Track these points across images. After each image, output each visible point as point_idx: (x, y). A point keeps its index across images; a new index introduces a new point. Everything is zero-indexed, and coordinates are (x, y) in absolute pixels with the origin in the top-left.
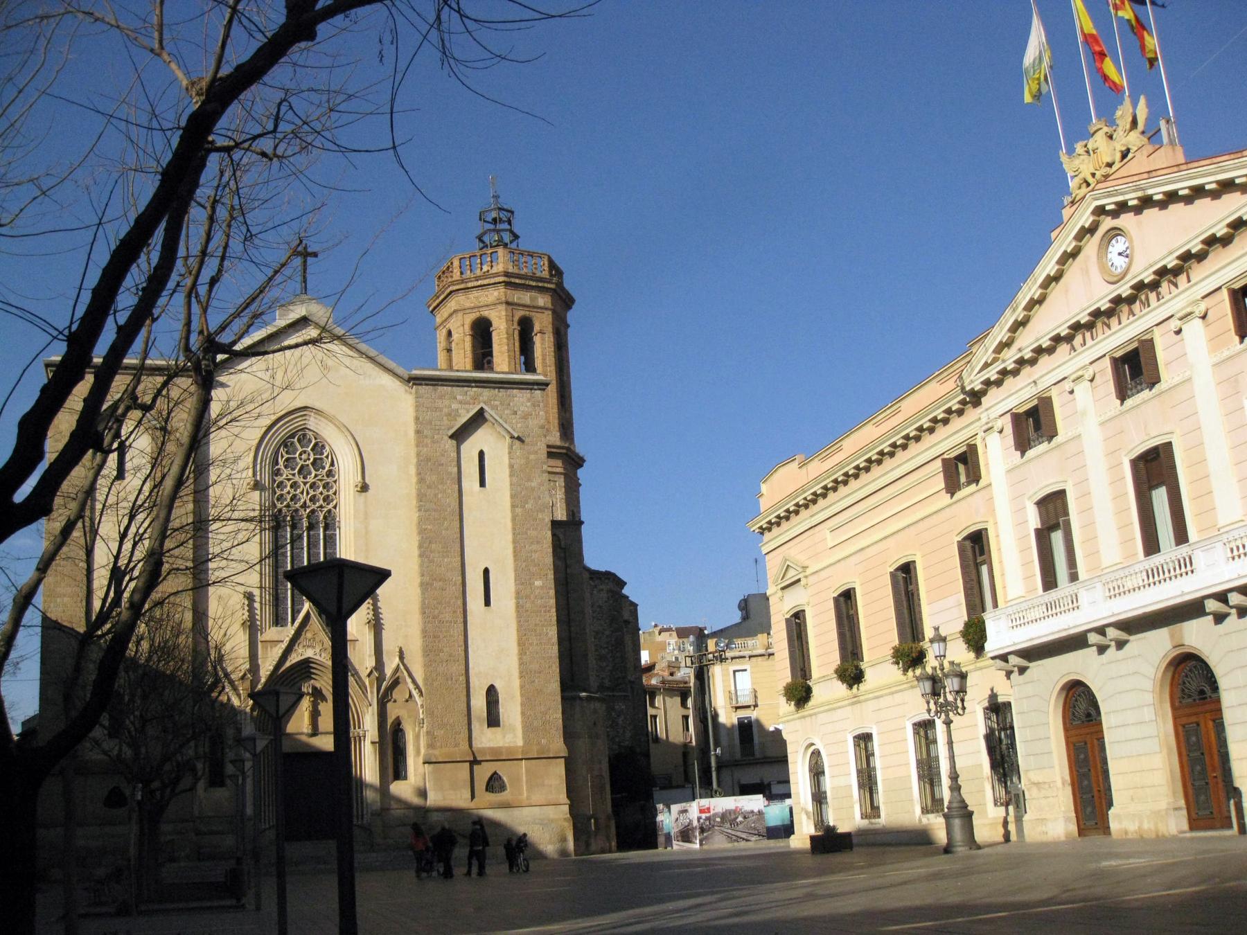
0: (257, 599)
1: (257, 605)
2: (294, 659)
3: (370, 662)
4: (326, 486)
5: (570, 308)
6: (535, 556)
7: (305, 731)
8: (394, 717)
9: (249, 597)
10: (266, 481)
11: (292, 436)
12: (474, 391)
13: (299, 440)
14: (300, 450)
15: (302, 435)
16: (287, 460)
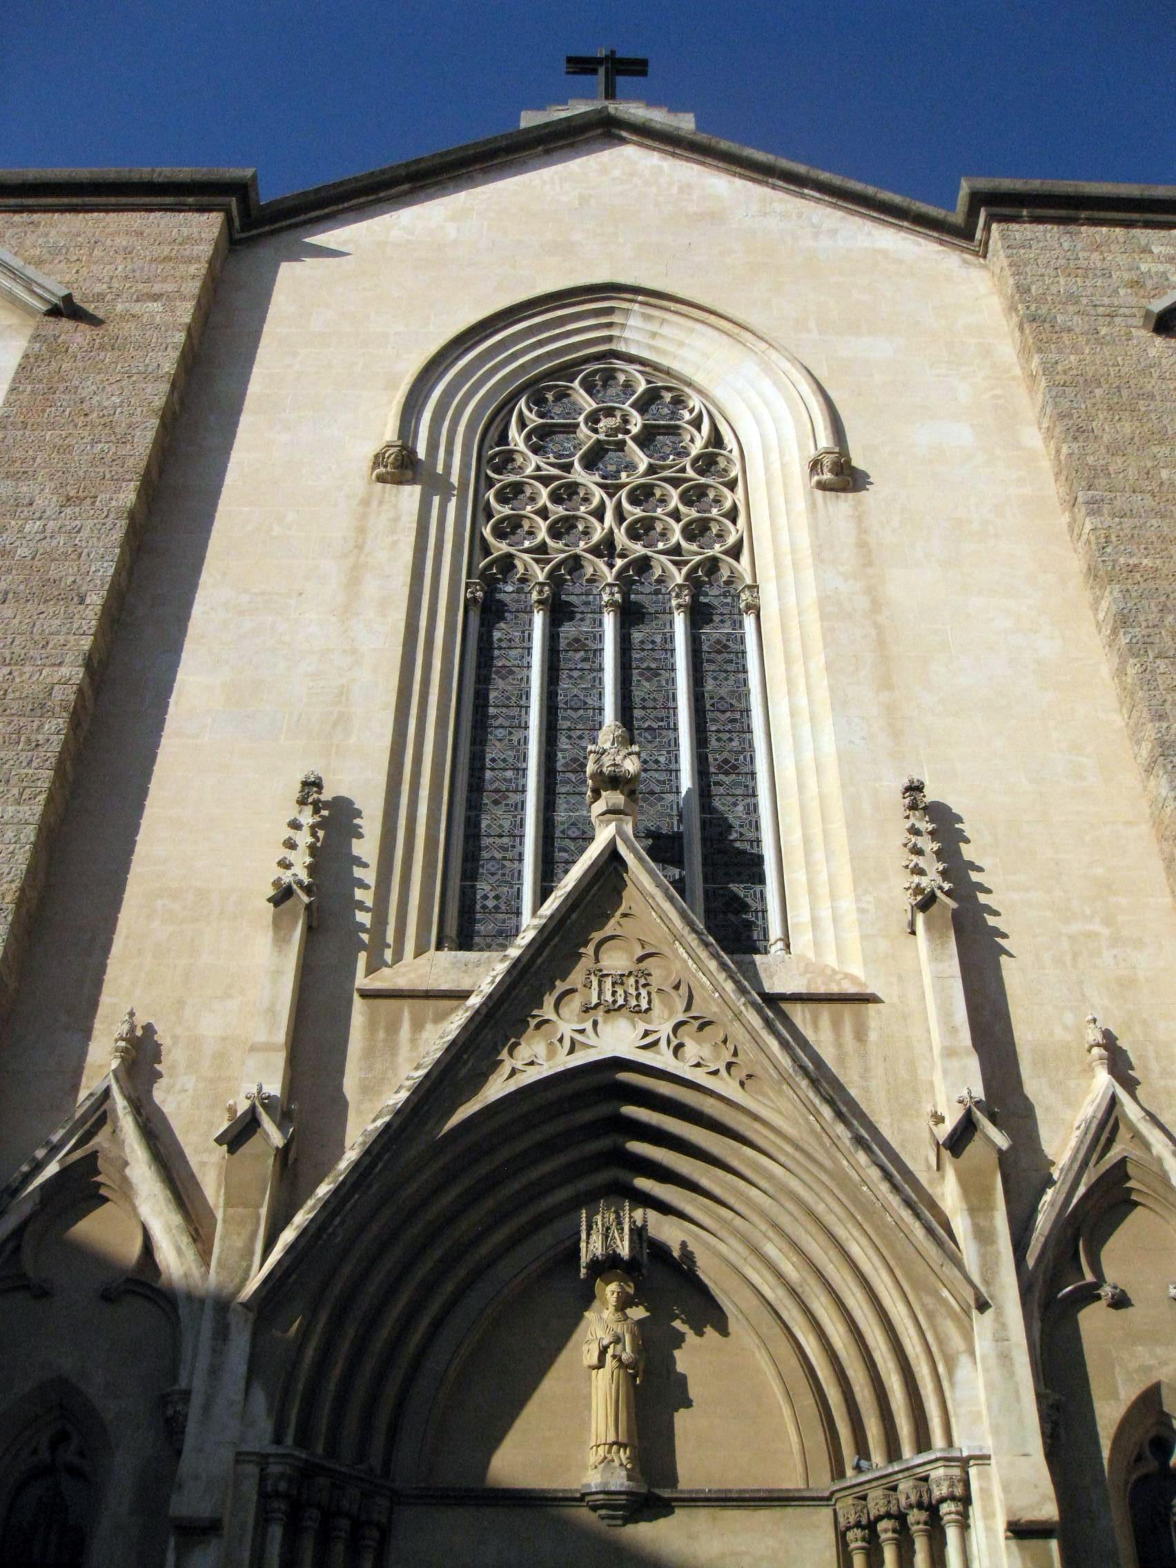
0: (371, 825)
1: (366, 847)
2: (534, 1060)
3: (954, 1083)
7: (593, 1479)
8: (1128, 1394)
9: (336, 820)
10: (455, 464)
11: (567, 371)
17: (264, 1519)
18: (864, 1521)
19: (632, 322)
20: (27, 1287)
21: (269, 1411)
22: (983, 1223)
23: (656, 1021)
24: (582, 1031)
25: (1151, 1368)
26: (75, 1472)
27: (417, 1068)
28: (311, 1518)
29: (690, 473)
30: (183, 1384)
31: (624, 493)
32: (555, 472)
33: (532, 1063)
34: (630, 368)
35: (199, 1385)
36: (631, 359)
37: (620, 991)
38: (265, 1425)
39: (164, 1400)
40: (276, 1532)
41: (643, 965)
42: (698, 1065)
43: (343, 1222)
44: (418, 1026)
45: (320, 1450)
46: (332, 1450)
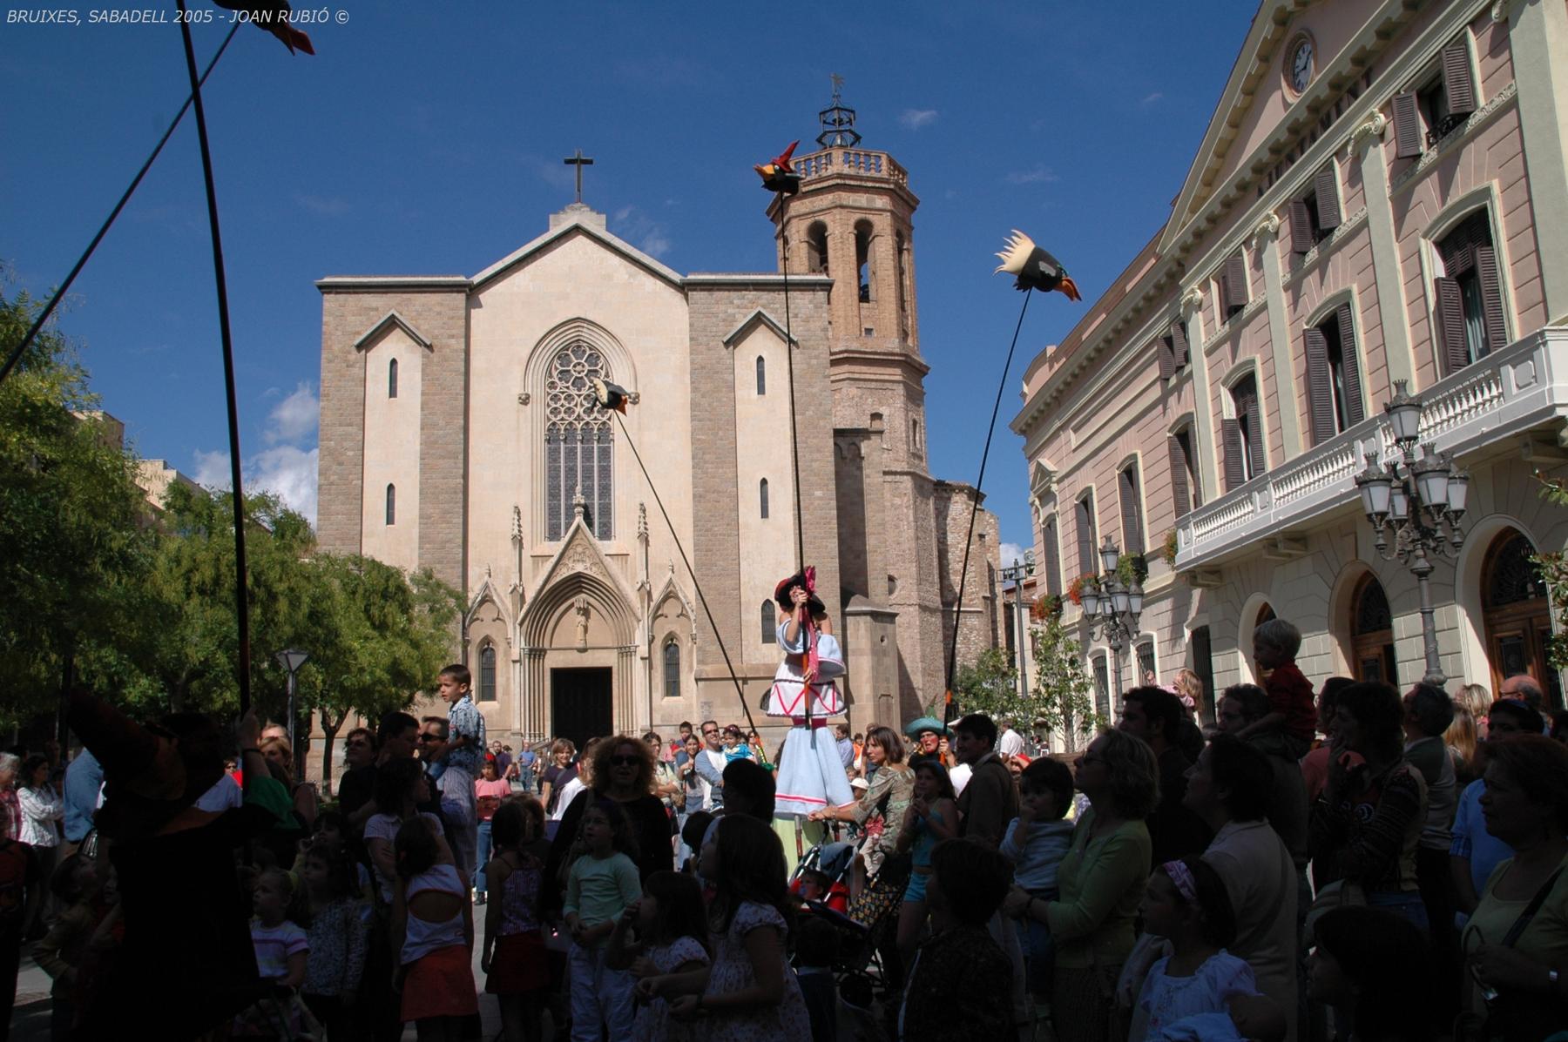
2: (564, 573)
5: (914, 209)
6: (815, 465)
12: (751, 295)
15: (577, 346)
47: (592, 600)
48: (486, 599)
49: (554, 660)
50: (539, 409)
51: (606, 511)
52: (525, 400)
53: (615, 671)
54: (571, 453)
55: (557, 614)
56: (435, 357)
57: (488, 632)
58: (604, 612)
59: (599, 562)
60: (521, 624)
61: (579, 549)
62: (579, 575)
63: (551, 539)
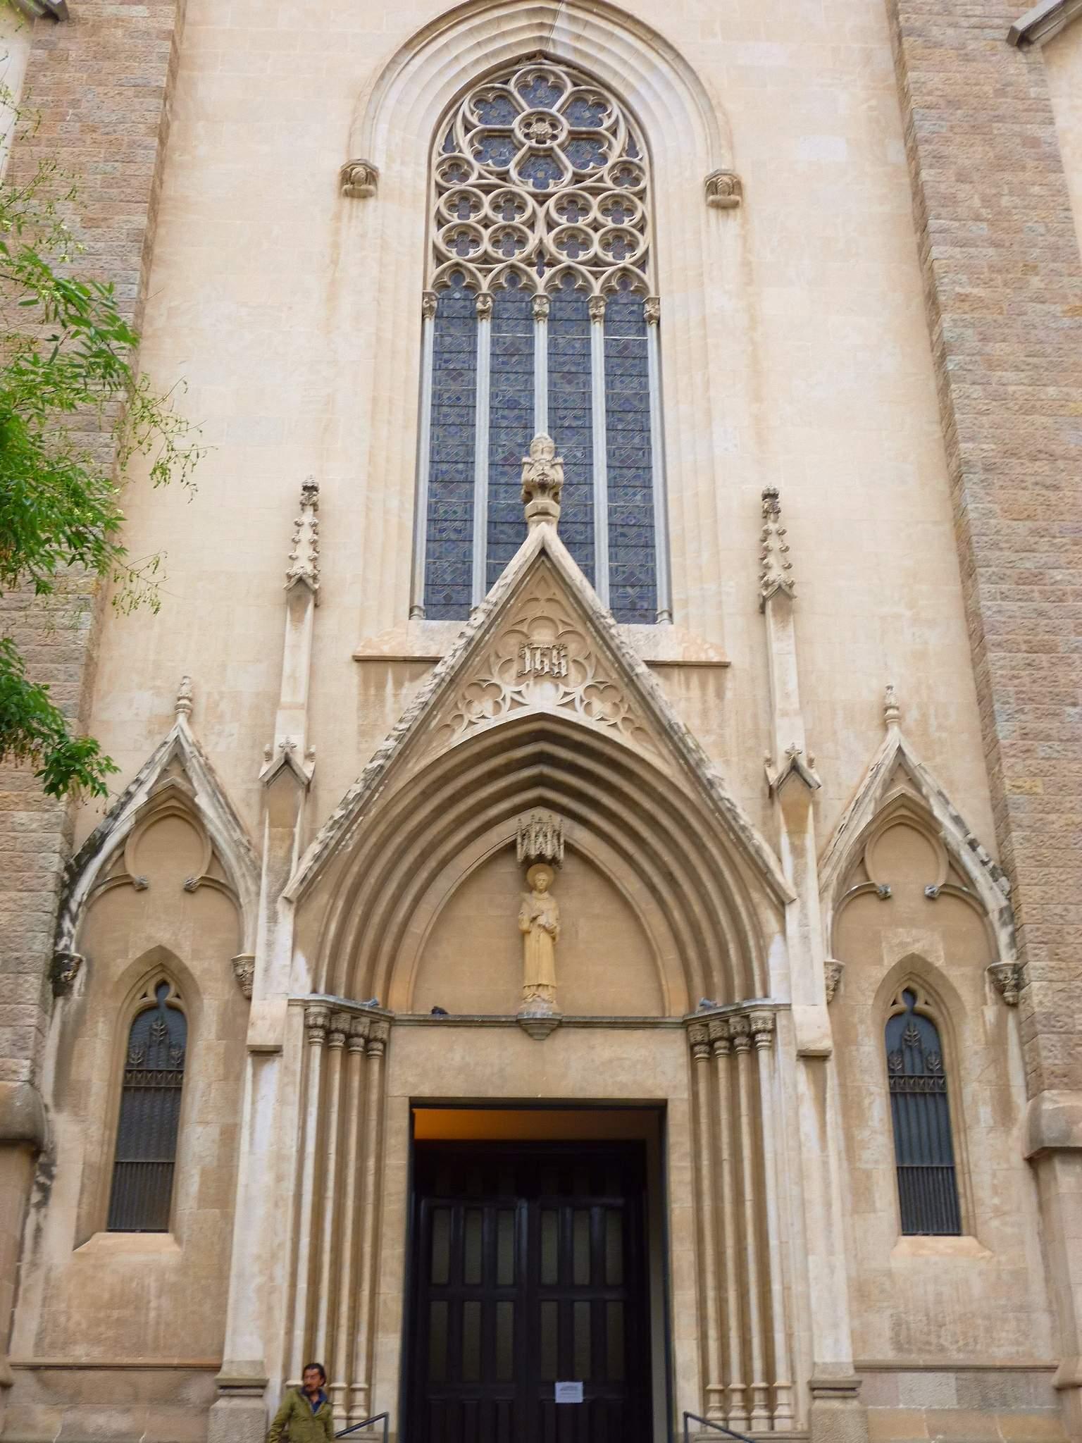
2: (485, 716)
4: (617, 207)
13: (524, 88)
14: (528, 110)
16: (487, 137)
17: (308, 1042)
18: (706, 1039)
19: (560, 23)
20: (131, 883)
21: (308, 970)
22: (797, 843)
23: (572, 684)
24: (519, 693)
25: (907, 944)
26: (173, 1008)
27: (401, 721)
28: (339, 1040)
29: (609, 183)
30: (247, 953)
31: (551, 202)
32: (493, 180)
33: (483, 717)
34: (559, 69)
35: (260, 955)
36: (558, 61)
37: (546, 661)
38: (306, 980)
39: (235, 963)
40: (317, 1050)
41: (563, 640)
42: (602, 719)
43: (351, 838)
44: (399, 684)
45: (342, 997)
46: (349, 995)
47: (583, 838)
48: (172, 806)
49: (435, 1065)
50: (403, 227)
51: (636, 535)
52: (358, 182)
53: (678, 1117)
54: (512, 358)
55: (446, 884)
56: (71, 42)
57: (163, 936)
58: (631, 885)
59: (622, 680)
60: (300, 902)
61: (543, 636)
62: (543, 730)
63: (429, 616)
